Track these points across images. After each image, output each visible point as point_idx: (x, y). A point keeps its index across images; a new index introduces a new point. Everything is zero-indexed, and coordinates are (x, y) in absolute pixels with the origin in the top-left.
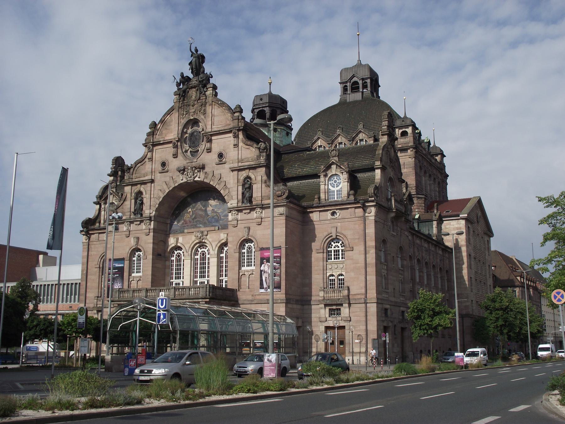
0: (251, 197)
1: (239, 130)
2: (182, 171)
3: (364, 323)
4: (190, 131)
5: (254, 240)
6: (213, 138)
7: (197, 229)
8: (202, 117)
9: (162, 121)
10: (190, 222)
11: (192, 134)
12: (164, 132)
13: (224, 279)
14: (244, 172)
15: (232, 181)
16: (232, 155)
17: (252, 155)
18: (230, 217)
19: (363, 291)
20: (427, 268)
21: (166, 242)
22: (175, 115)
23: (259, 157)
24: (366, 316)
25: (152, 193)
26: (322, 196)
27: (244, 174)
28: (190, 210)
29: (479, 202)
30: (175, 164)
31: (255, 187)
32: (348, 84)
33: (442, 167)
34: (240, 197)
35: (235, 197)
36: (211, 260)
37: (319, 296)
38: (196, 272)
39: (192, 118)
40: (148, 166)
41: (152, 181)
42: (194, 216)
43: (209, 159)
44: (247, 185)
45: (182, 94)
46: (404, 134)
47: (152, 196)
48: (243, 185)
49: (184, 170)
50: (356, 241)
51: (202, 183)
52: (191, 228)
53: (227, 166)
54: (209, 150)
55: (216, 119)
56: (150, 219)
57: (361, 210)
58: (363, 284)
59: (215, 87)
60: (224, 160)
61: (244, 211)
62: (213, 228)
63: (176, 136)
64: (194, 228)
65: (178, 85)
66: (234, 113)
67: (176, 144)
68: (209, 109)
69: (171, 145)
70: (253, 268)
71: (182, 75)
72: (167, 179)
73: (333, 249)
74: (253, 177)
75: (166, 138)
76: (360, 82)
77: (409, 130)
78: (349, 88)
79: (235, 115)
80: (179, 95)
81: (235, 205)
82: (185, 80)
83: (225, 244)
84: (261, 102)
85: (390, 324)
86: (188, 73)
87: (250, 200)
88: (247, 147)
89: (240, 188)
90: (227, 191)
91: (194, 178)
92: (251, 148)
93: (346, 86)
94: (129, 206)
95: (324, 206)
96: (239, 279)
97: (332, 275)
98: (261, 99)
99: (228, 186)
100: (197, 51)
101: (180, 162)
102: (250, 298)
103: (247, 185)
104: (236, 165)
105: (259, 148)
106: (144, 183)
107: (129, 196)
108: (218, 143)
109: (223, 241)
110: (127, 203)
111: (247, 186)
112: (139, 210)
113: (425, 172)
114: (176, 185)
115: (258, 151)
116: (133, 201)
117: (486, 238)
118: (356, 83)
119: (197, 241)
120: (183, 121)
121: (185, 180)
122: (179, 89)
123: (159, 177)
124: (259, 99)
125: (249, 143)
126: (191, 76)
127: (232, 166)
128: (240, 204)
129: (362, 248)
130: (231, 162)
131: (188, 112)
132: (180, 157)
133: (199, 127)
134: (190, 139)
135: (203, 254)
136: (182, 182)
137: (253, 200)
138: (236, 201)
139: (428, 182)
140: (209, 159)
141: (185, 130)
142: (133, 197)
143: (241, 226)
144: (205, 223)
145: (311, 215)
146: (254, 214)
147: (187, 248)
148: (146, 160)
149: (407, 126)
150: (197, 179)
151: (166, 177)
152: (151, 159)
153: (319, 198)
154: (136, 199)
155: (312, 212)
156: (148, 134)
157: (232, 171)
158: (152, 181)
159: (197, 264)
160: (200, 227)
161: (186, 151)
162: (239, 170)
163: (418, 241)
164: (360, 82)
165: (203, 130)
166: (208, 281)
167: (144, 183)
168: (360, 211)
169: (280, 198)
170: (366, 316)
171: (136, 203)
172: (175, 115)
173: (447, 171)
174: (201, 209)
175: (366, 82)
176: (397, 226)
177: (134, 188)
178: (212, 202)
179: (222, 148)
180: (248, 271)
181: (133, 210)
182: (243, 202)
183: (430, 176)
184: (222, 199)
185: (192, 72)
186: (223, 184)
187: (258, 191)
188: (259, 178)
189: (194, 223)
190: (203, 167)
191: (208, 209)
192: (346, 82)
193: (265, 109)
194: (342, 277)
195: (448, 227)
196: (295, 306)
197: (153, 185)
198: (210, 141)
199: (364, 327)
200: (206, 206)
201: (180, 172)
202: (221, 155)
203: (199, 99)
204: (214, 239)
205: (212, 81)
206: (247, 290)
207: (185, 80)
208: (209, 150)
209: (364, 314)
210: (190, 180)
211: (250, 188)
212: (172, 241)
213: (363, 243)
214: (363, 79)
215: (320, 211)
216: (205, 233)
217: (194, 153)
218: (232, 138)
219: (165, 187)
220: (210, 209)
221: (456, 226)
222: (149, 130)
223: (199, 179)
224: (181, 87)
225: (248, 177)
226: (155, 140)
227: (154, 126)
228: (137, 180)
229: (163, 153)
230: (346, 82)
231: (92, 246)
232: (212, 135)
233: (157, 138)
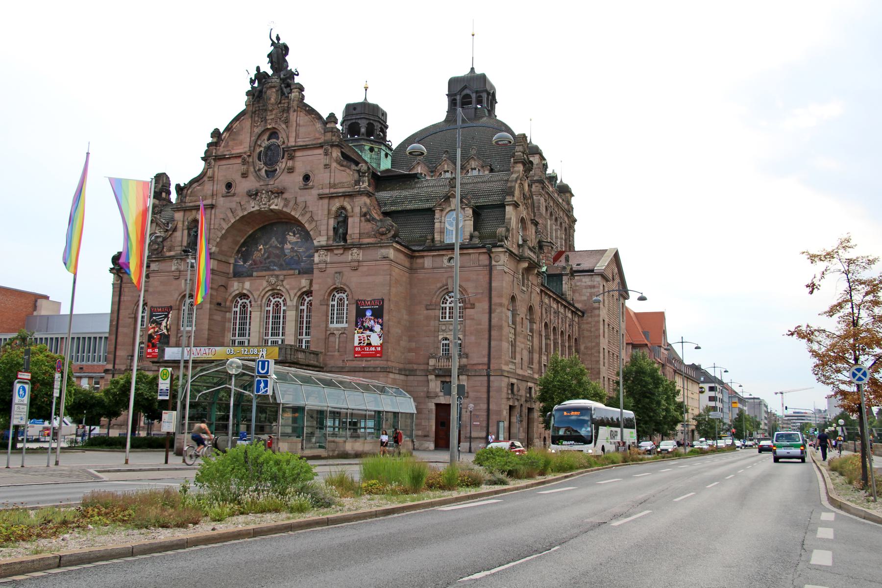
0: (345, 234)
1: (332, 146)
2: (253, 195)
3: (485, 401)
4: (266, 143)
5: (347, 289)
6: (298, 154)
7: (271, 273)
8: (284, 126)
9: (228, 129)
10: (261, 263)
11: (268, 148)
12: (231, 143)
13: (305, 338)
14: (337, 200)
16: (322, 178)
17: (349, 179)
18: (316, 259)
19: (486, 360)
20: (555, 334)
21: (225, 287)
22: (247, 123)
23: (357, 182)
24: (488, 392)
25: (212, 222)
26: (437, 237)
27: (337, 204)
28: (261, 247)
29: (616, 256)
30: (243, 186)
31: (350, 220)
32: (458, 98)
33: (568, 210)
34: (331, 233)
35: (324, 232)
36: (288, 313)
37: (428, 364)
38: (301, 328)
39: (269, 127)
40: (208, 188)
42: (266, 255)
44: (342, 219)
45: (256, 96)
47: (212, 227)
48: (336, 217)
49: (256, 194)
50: (479, 296)
51: (280, 212)
52: (262, 271)
53: (315, 192)
54: (291, 170)
55: (302, 130)
57: (486, 257)
58: (485, 352)
59: (301, 89)
60: (311, 184)
61: (336, 252)
62: (291, 272)
63: (247, 149)
64: (265, 270)
65: (252, 82)
68: (293, 116)
69: (239, 161)
70: (345, 325)
71: (258, 69)
72: (233, 205)
73: (448, 305)
74: (349, 207)
75: (233, 152)
76: (474, 96)
78: (458, 102)
80: (254, 95)
81: (324, 243)
82: (260, 76)
83: (309, 293)
84: (354, 112)
85: (516, 404)
86: (267, 68)
88: (342, 168)
89: (332, 222)
90: (314, 224)
91: (270, 206)
92: (348, 171)
93: (455, 100)
94: (180, 239)
95: (439, 250)
96: (327, 339)
97: (446, 339)
98: (355, 109)
99: (315, 218)
100: (278, 38)
101: (251, 184)
102: (340, 364)
103: (342, 219)
104: (327, 191)
105: (359, 171)
107: (180, 225)
108: (304, 162)
109: (304, 290)
110: (178, 234)
111: (341, 219)
113: (551, 214)
114: (245, 213)
115: (356, 175)
116: (186, 232)
117: (622, 300)
118: (468, 96)
119: (270, 288)
120: (257, 130)
121: (257, 208)
122: (253, 88)
123: (221, 201)
124: (352, 109)
125: (345, 163)
126: (270, 72)
127: (321, 191)
128: (331, 242)
129: (486, 306)
131: (265, 120)
132: (251, 177)
133: (278, 138)
134: (266, 155)
135: (277, 305)
136: (253, 210)
137: (348, 237)
138: (325, 238)
139: (554, 227)
140: (292, 182)
141: (259, 143)
142: (185, 227)
143: (331, 270)
144: (281, 265)
145: (420, 261)
147: (256, 297)
148: (206, 179)
150: (273, 207)
151: (232, 203)
152: (212, 178)
153: (433, 240)
154: (189, 229)
155: (423, 257)
156: (209, 145)
157: (321, 198)
158: (212, 207)
159: (268, 317)
160: (274, 270)
161: (259, 170)
162: (331, 197)
163: (546, 301)
164: (474, 96)
165: (284, 143)
166: (283, 341)
168: (484, 259)
169: (383, 237)
170: (488, 392)
171: (189, 234)
173: (576, 214)
174: (276, 247)
175: (481, 96)
176: (528, 280)
177: (188, 213)
178: (291, 238)
179: (309, 168)
180: (338, 329)
181: (185, 244)
182: (334, 240)
183: (556, 219)
184: (306, 236)
185: (272, 67)
186: (308, 216)
187: (355, 227)
188: (357, 210)
189: (265, 266)
191: (286, 246)
192: (455, 95)
193: (359, 121)
194: (447, 342)
195: (578, 284)
196: (397, 376)
197: (213, 211)
198: (292, 158)
199: (485, 406)
200: (284, 241)
201: (250, 196)
202: (307, 178)
203: (280, 103)
204: (293, 285)
205: (297, 80)
206: (336, 353)
207: (260, 76)
209: (485, 389)
210: (264, 208)
213: (487, 299)
214: (477, 92)
215: (433, 256)
216: (281, 277)
217: (271, 173)
218: (322, 156)
219: (230, 215)
220: (288, 246)
221: (589, 283)
222: (210, 140)
223: (276, 208)
224: (256, 85)
225: (343, 208)
226: (219, 153)
227: (216, 133)
228: (191, 204)
229: (229, 171)
230: (455, 95)
231: (126, 290)
232: (294, 151)
233: (221, 150)
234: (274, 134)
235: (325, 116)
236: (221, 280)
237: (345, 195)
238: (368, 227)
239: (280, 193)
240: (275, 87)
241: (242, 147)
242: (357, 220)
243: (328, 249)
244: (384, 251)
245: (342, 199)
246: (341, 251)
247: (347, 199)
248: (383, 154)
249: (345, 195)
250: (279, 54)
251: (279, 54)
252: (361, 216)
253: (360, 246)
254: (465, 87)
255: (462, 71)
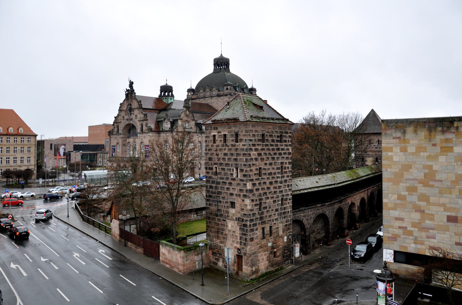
2: (127, 120)
4: (129, 107)
16: (138, 116)
21: (126, 140)
22: (126, 102)
27: (141, 122)
41: (121, 122)
43: (133, 116)
45: (127, 95)
46: (227, 89)
53: (138, 119)
54: (133, 114)
56: (120, 134)
59: (135, 93)
67: (126, 111)
77: (229, 87)
82: (128, 90)
106: (118, 123)
112: (118, 130)
146: (144, 135)
149: (228, 86)
167: (118, 123)
172: (126, 102)
187: (144, 128)
190: (132, 119)
198: (133, 111)
202: (136, 116)
208: (133, 114)
211: (142, 127)
212: (128, 141)
227: (121, 104)
234: (131, 105)
235: (139, 100)
236: (124, 139)
237: (142, 121)
238: (146, 128)
239: (132, 119)
240: (130, 93)
241: (125, 108)
243: (140, 133)
244: (149, 134)
248: (169, 99)
249: (142, 121)
250: (131, 84)
251: (131, 84)
253: (145, 133)
254: (217, 62)
255: (218, 56)
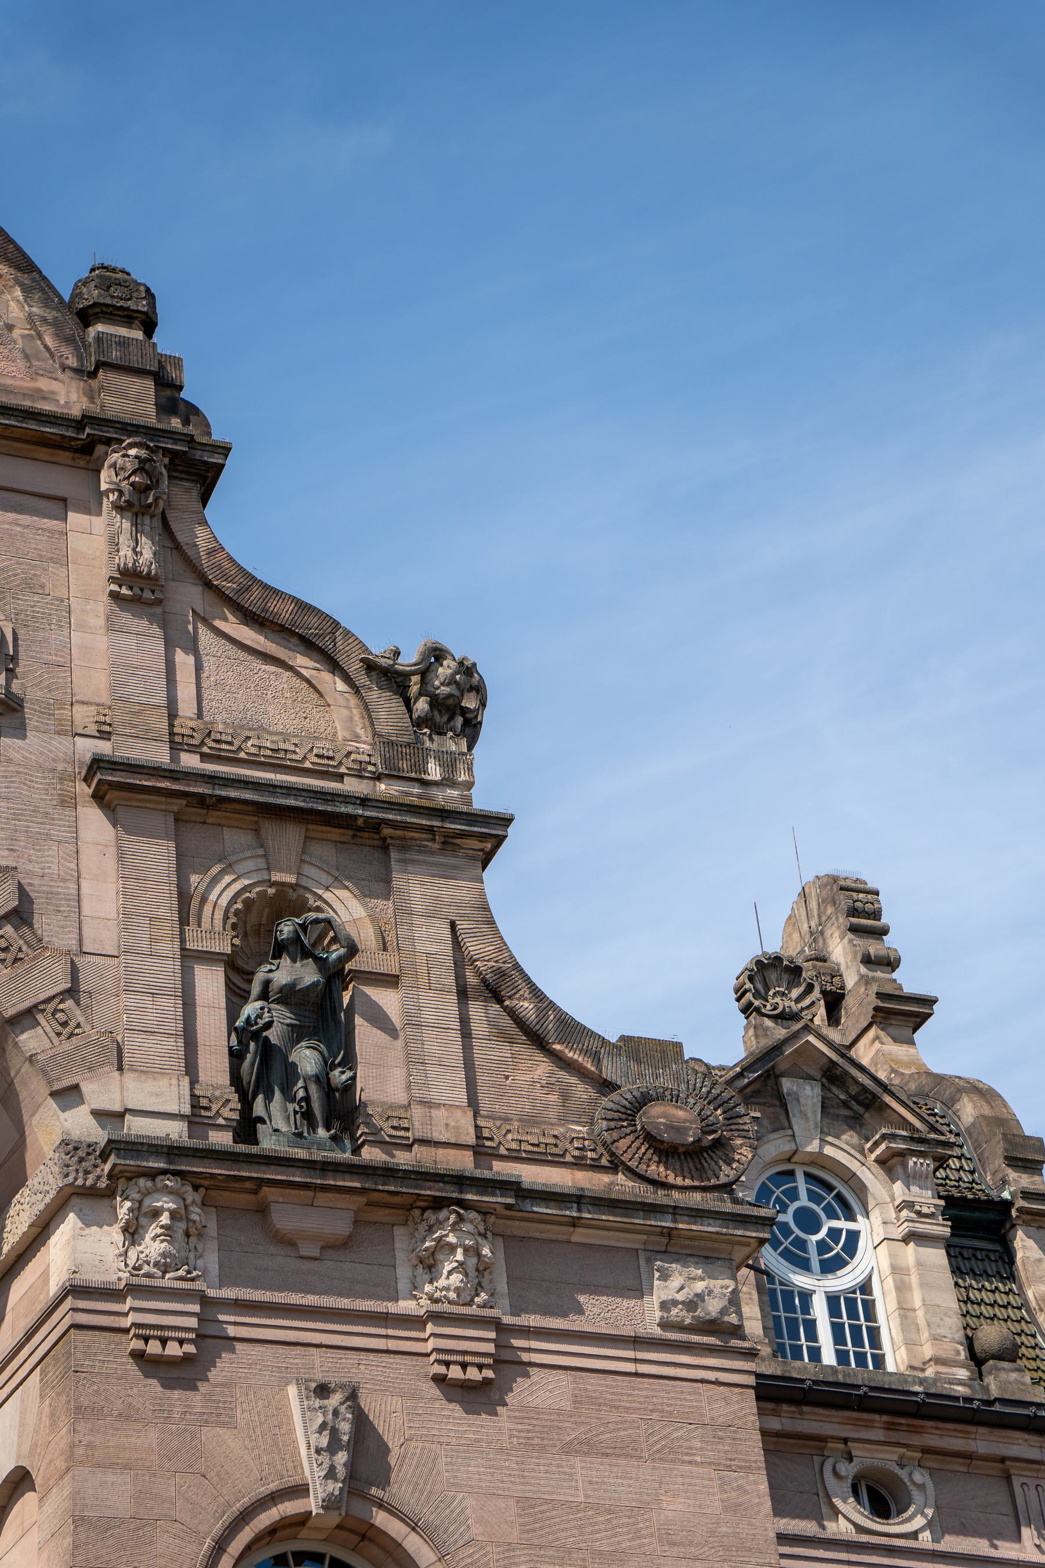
15: (102, 900)
23: (398, 759)
34: (215, 1069)
61: (288, 1216)
66: (86, 317)
79: (100, 327)
81: (175, 1131)
87: (342, 1110)
89: (210, 985)
92: (302, 661)
104: (160, 755)
130: (83, 716)
138: (172, 1094)
188: (431, 941)
211: (324, 1014)
242: (440, 1007)
245: (287, 838)
246: (330, 1220)
247: (323, 851)
252: (463, 994)
